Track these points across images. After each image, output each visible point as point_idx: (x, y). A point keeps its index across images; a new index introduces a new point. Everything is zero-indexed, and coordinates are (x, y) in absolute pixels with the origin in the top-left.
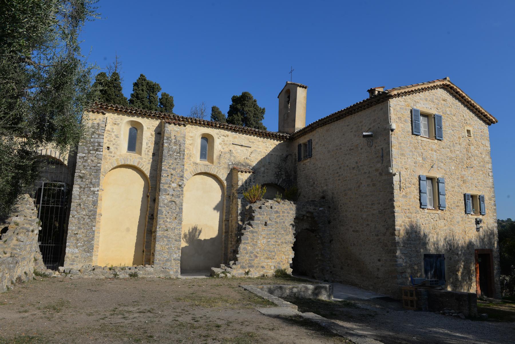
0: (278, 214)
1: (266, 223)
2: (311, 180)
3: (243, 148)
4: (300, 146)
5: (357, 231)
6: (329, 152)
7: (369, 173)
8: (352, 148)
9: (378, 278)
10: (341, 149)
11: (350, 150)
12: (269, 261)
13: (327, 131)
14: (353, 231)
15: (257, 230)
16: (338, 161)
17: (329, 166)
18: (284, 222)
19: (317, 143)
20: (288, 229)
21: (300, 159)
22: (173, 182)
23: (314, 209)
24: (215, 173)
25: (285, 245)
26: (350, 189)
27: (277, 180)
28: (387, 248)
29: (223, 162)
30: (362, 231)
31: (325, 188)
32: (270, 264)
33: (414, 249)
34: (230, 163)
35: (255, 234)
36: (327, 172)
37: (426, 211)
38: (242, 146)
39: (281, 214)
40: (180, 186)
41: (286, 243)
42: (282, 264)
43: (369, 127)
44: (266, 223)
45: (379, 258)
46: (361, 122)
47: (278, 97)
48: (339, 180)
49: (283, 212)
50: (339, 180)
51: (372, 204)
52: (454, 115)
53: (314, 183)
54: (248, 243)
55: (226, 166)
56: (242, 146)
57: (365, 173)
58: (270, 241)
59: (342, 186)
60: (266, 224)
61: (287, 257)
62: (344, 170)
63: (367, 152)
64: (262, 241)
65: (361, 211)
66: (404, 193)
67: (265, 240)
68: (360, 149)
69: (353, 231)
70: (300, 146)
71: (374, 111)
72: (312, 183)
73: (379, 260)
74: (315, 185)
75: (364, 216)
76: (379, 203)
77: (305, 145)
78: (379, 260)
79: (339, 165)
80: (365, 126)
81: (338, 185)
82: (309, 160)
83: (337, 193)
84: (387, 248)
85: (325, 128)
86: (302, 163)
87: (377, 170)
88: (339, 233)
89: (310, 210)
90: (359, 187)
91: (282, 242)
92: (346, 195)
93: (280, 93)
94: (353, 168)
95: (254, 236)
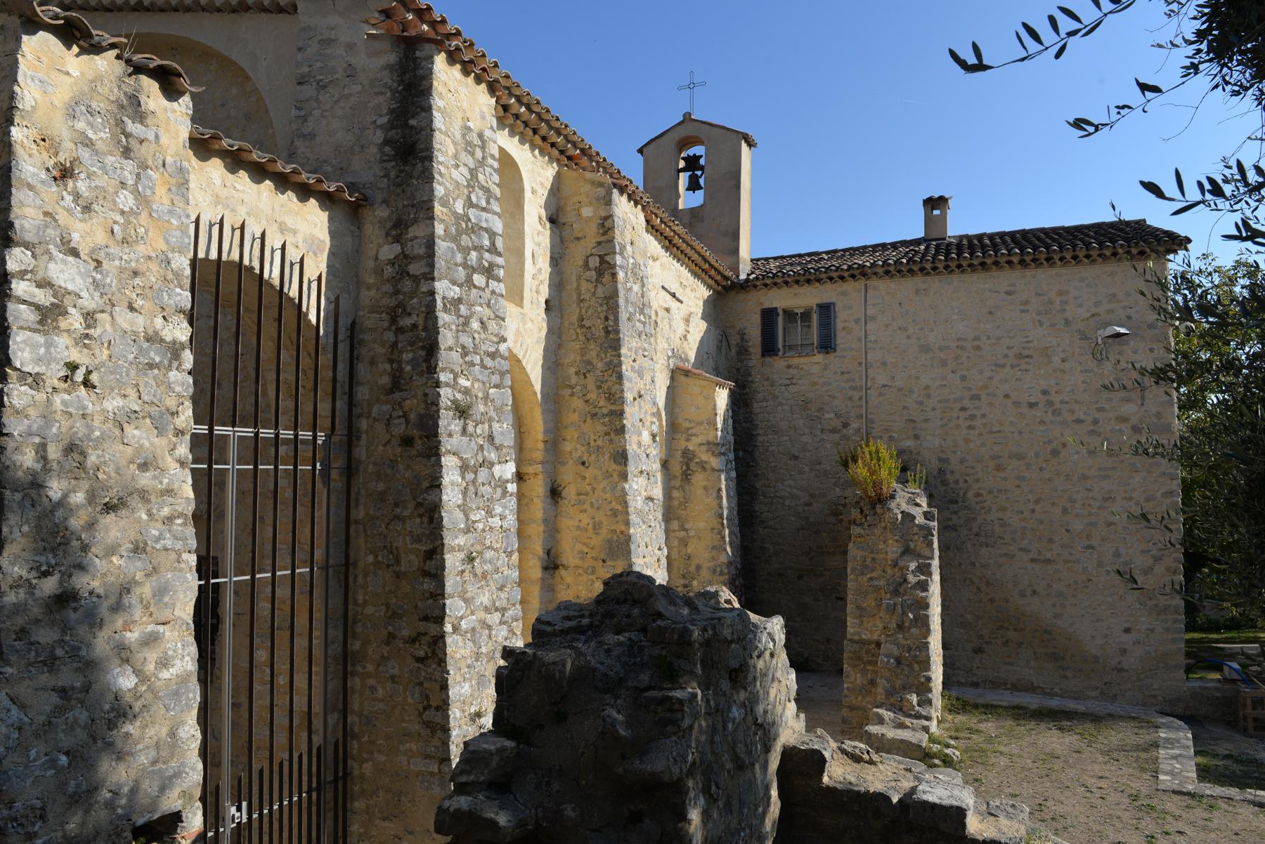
4: (769, 316)
5: (1048, 561)
7: (1095, 422)
8: (1025, 353)
9: (1120, 670)
11: (1020, 356)
13: (917, 291)
14: (1033, 560)
16: (963, 378)
17: (927, 387)
21: (769, 348)
26: (1020, 457)
28: (1154, 602)
30: (1067, 562)
31: (909, 443)
36: (921, 403)
43: (1094, 310)
45: (1127, 625)
47: (640, 151)
48: (970, 427)
50: (970, 427)
51: (1106, 499)
57: (1079, 421)
59: (983, 444)
62: (991, 404)
63: (1086, 371)
65: (1065, 511)
68: (1056, 359)
69: (1033, 560)
70: (769, 316)
71: (1112, 274)
73: (1127, 631)
74: (849, 431)
75: (1078, 526)
76: (1130, 499)
77: (790, 315)
78: (1127, 631)
79: (969, 389)
80: (1080, 306)
81: (967, 441)
82: (819, 358)
83: (962, 461)
84: (1154, 602)
86: (778, 363)
87: (1123, 419)
88: (973, 564)
90: (1055, 453)
92: (999, 468)
93: (653, 140)
94: (1032, 405)
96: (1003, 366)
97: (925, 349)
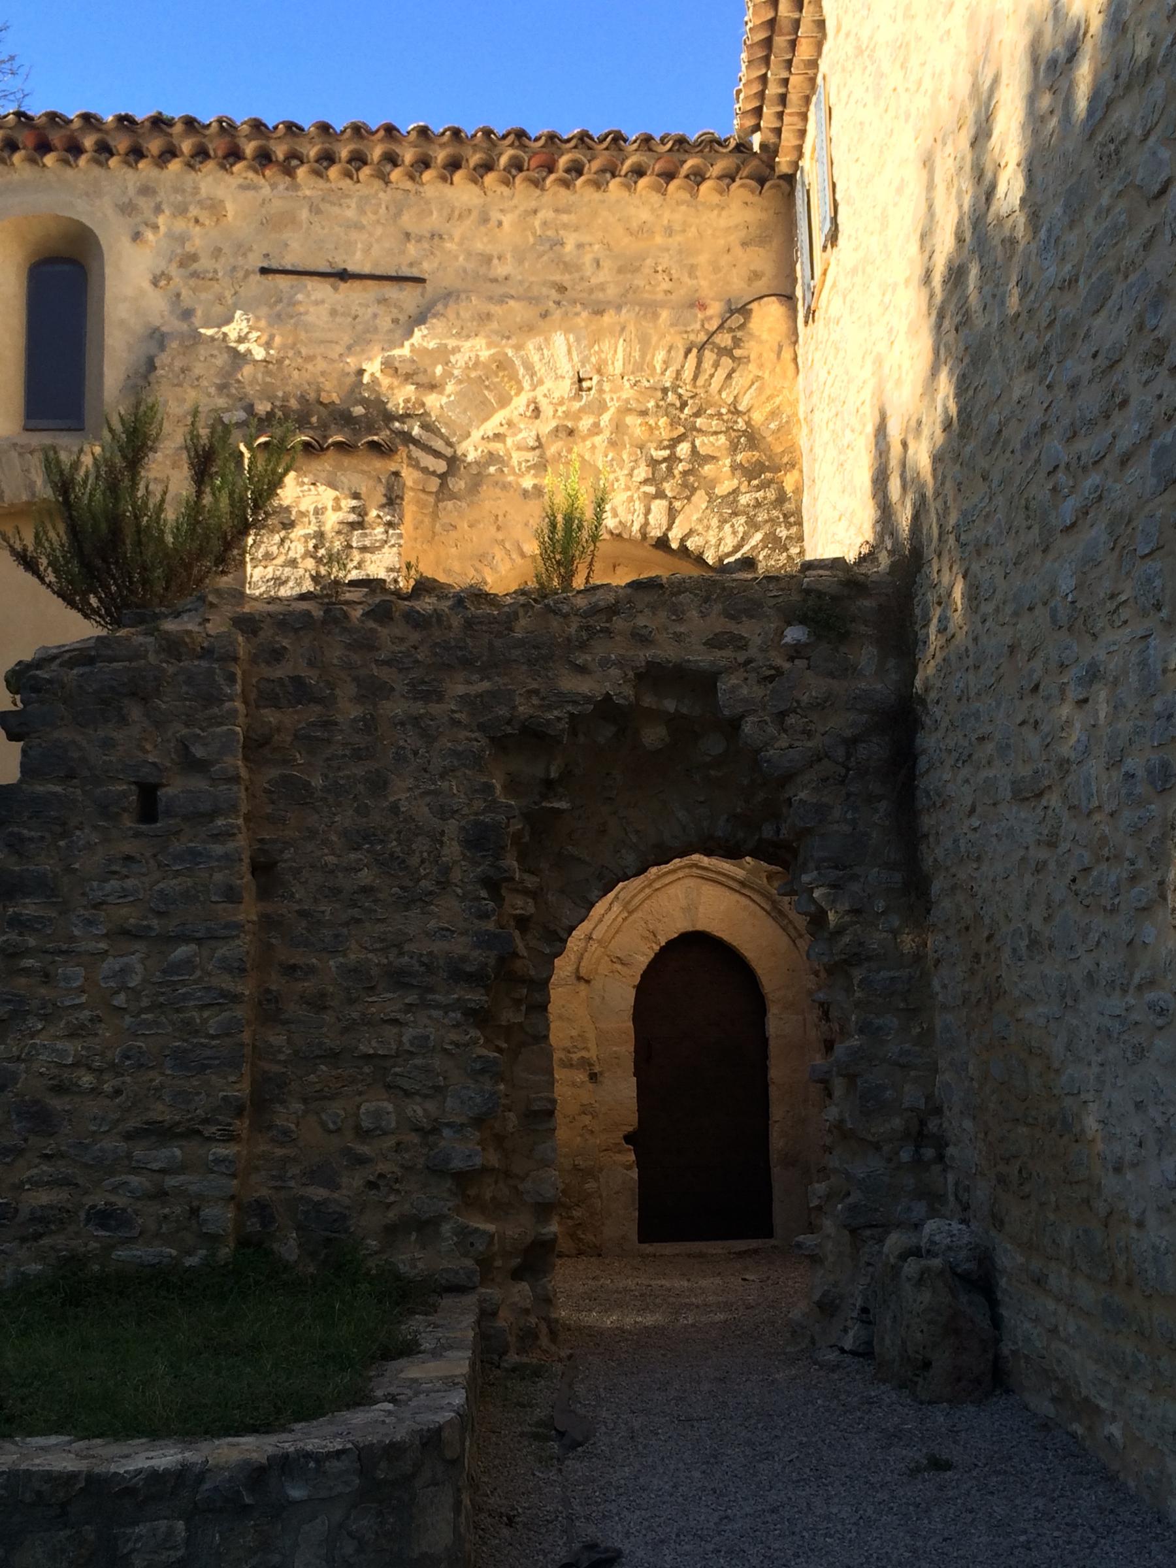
0: (314, 712)
1: (148, 793)
3: (353, 295)
15: (47, 865)
18: (378, 785)
20: (421, 845)
23: (714, 643)
25: (388, 1002)
27: (659, 508)
32: (192, 1182)
35: (30, 908)
38: (343, 275)
39: (349, 710)
41: (399, 979)
56: (343, 275)
58: (187, 964)
60: (148, 803)
61: (417, 1110)
64: (111, 964)
67: (136, 962)
89: (666, 652)
91: (355, 972)
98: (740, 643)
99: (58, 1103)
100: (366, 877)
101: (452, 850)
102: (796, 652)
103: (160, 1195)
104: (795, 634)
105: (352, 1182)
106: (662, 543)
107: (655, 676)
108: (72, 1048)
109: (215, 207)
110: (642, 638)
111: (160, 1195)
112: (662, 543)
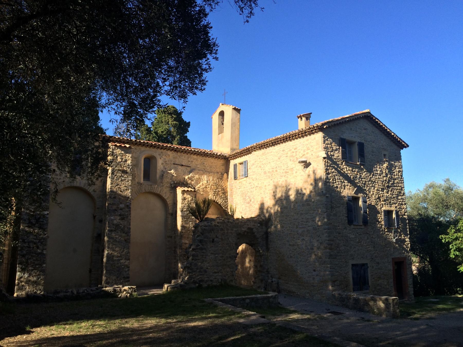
1: (213, 240)
2: (247, 198)
3: (183, 168)
6: (265, 173)
8: (287, 171)
9: (314, 286)
10: (276, 171)
12: (217, 274)
17: (266, 186)
19: (253, 164)
22: (121, 203)
24: (158, 193)
27: (214, 198)
28: (321, 260)
29: (166, 181)
33: (344, 260)
34: (172, 183)
35: (204, 251)
37: (352, 226)
39: (226, 231)
40: (127, 206)
41: (230, 257)
42: (227, 277)
43: (303, 153)
44: (213, 240)
45: (314, 268)
46: (295, 149)
49: (228, 230)
52: (373, 142)
53: (251, 201)
54: (198, 260)
55: (169, 185)
56: (182, 165)
58: (217, 257)
60: (213, 241)
65: (297, 227)
66: (334, 212)
72: (249, 200)
74: (251, 203)
78: (314, 271)
85: (263, 151)
95: (203, 252)
96: (282, 176)
97: (265, 173)
98: (255, 226)
99: (207, 270)
100: (228, 248)
101: (234, 245)
102: (259, 227)
103: (215, 278)
104: (259, 225)
105: (227, 277)
106: (215, 201)
107: (249, 228)
108: (208, 265)
109: (169, 155)
110: (248, 225)
111: (215, 278)
112: (215, 201)
